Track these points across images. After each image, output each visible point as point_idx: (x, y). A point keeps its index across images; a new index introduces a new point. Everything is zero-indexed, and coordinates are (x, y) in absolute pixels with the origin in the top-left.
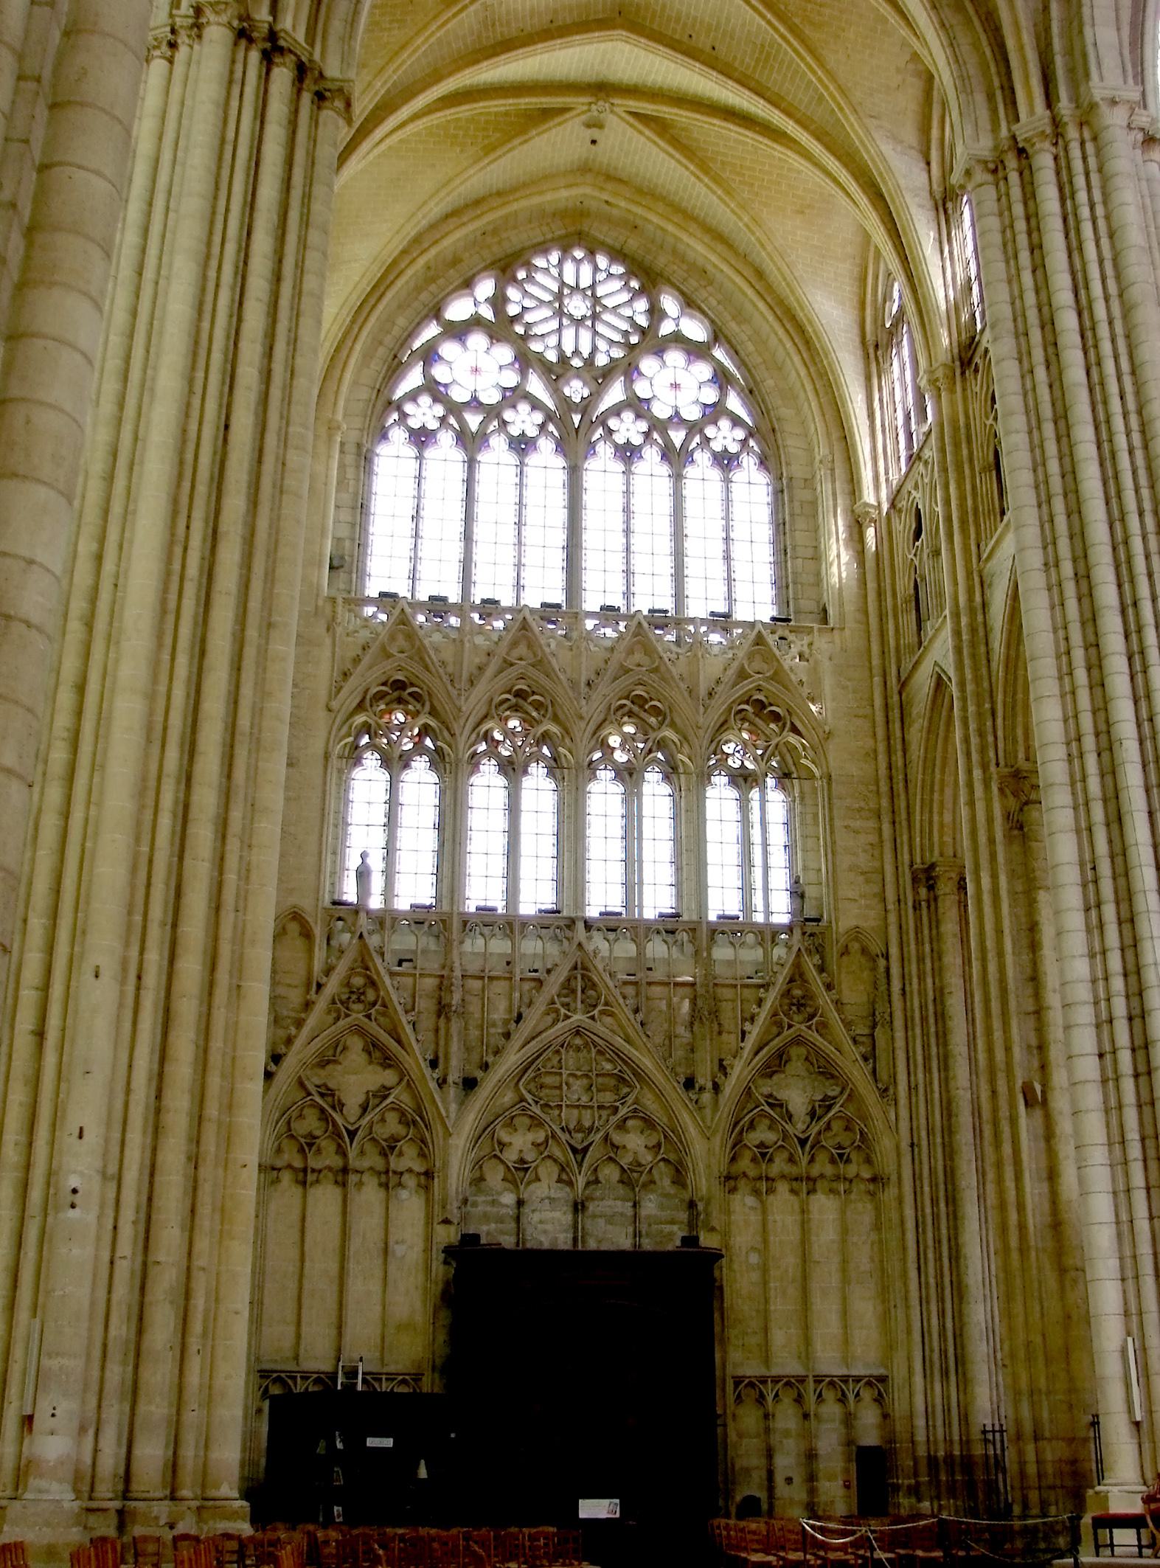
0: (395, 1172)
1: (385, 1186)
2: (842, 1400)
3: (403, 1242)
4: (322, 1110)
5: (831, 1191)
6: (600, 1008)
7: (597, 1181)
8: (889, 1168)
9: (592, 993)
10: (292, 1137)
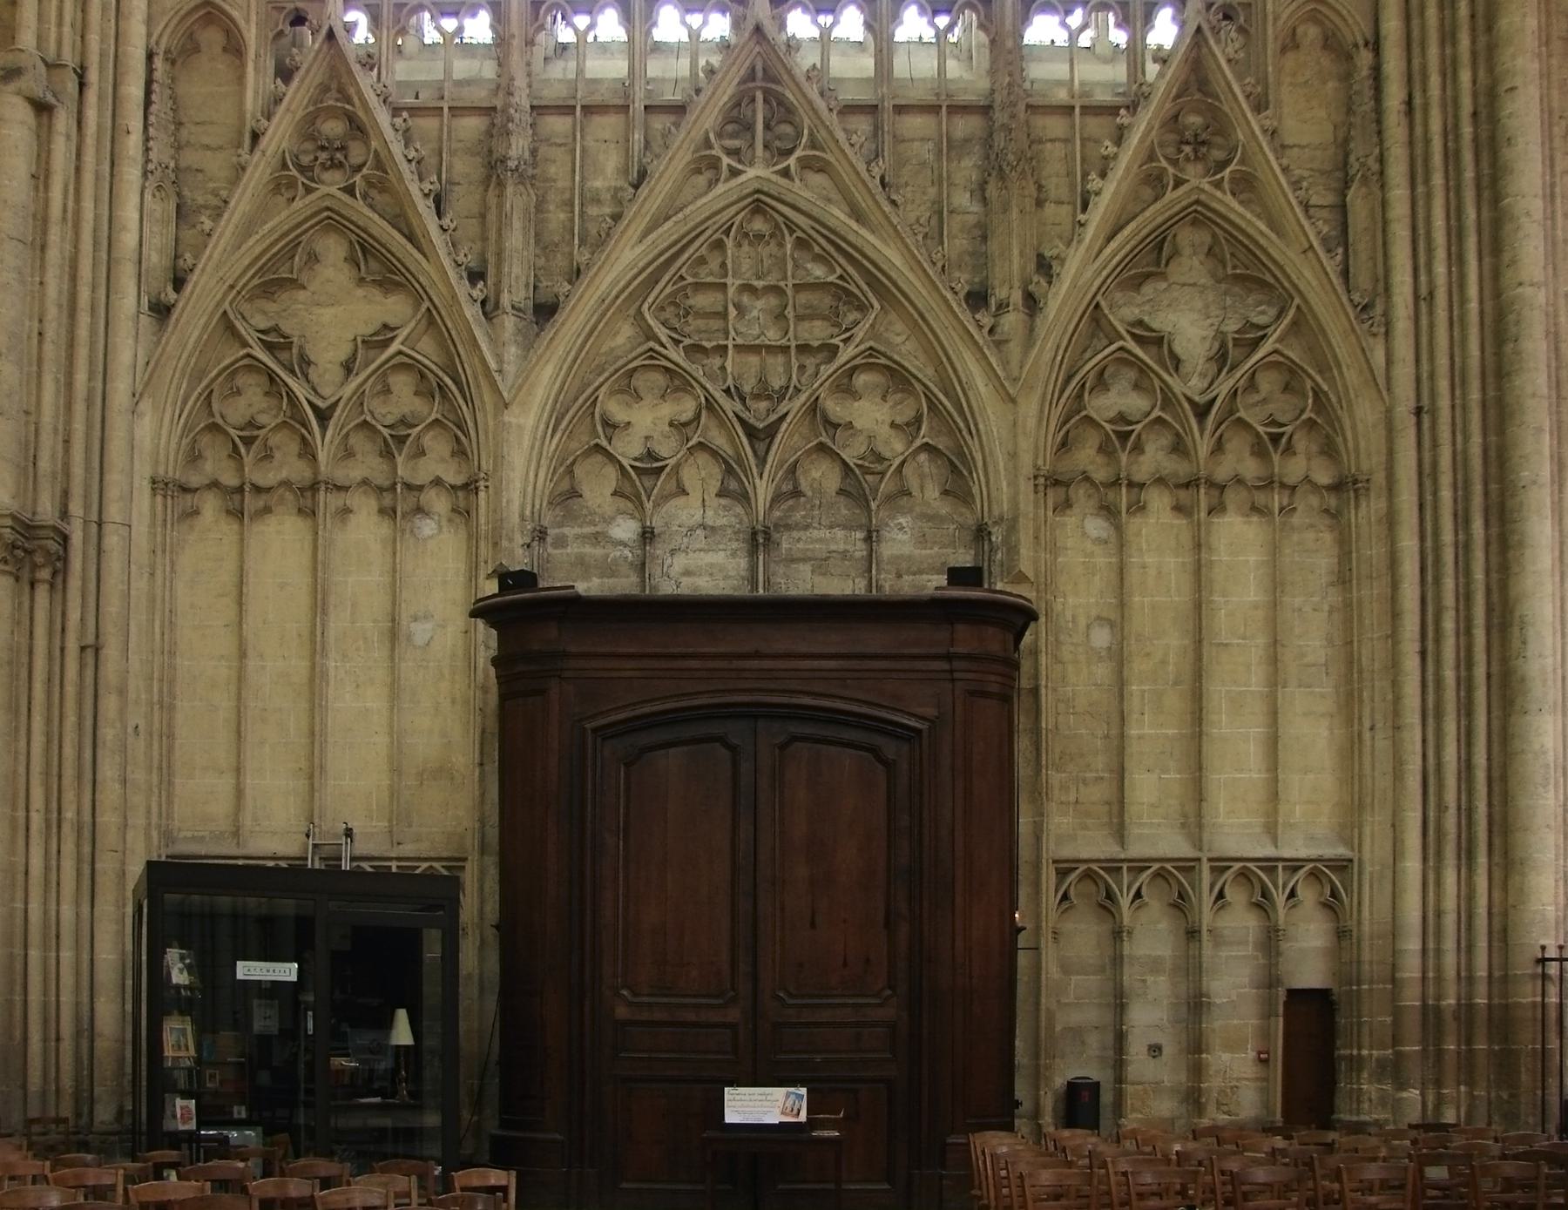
0: (409, 487)
1: (388, 512)
2: (1263, 904)
3: (427, 617)
4: (272, 377)
5: (1255, 509)
6: (798, 153)
7: (797, 493)
8: (1370, 460)
9: (786, 129)
10: (214, 428)
